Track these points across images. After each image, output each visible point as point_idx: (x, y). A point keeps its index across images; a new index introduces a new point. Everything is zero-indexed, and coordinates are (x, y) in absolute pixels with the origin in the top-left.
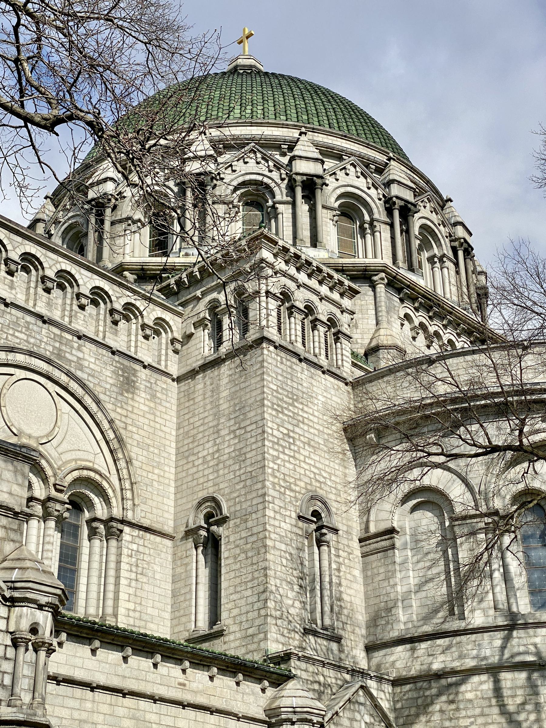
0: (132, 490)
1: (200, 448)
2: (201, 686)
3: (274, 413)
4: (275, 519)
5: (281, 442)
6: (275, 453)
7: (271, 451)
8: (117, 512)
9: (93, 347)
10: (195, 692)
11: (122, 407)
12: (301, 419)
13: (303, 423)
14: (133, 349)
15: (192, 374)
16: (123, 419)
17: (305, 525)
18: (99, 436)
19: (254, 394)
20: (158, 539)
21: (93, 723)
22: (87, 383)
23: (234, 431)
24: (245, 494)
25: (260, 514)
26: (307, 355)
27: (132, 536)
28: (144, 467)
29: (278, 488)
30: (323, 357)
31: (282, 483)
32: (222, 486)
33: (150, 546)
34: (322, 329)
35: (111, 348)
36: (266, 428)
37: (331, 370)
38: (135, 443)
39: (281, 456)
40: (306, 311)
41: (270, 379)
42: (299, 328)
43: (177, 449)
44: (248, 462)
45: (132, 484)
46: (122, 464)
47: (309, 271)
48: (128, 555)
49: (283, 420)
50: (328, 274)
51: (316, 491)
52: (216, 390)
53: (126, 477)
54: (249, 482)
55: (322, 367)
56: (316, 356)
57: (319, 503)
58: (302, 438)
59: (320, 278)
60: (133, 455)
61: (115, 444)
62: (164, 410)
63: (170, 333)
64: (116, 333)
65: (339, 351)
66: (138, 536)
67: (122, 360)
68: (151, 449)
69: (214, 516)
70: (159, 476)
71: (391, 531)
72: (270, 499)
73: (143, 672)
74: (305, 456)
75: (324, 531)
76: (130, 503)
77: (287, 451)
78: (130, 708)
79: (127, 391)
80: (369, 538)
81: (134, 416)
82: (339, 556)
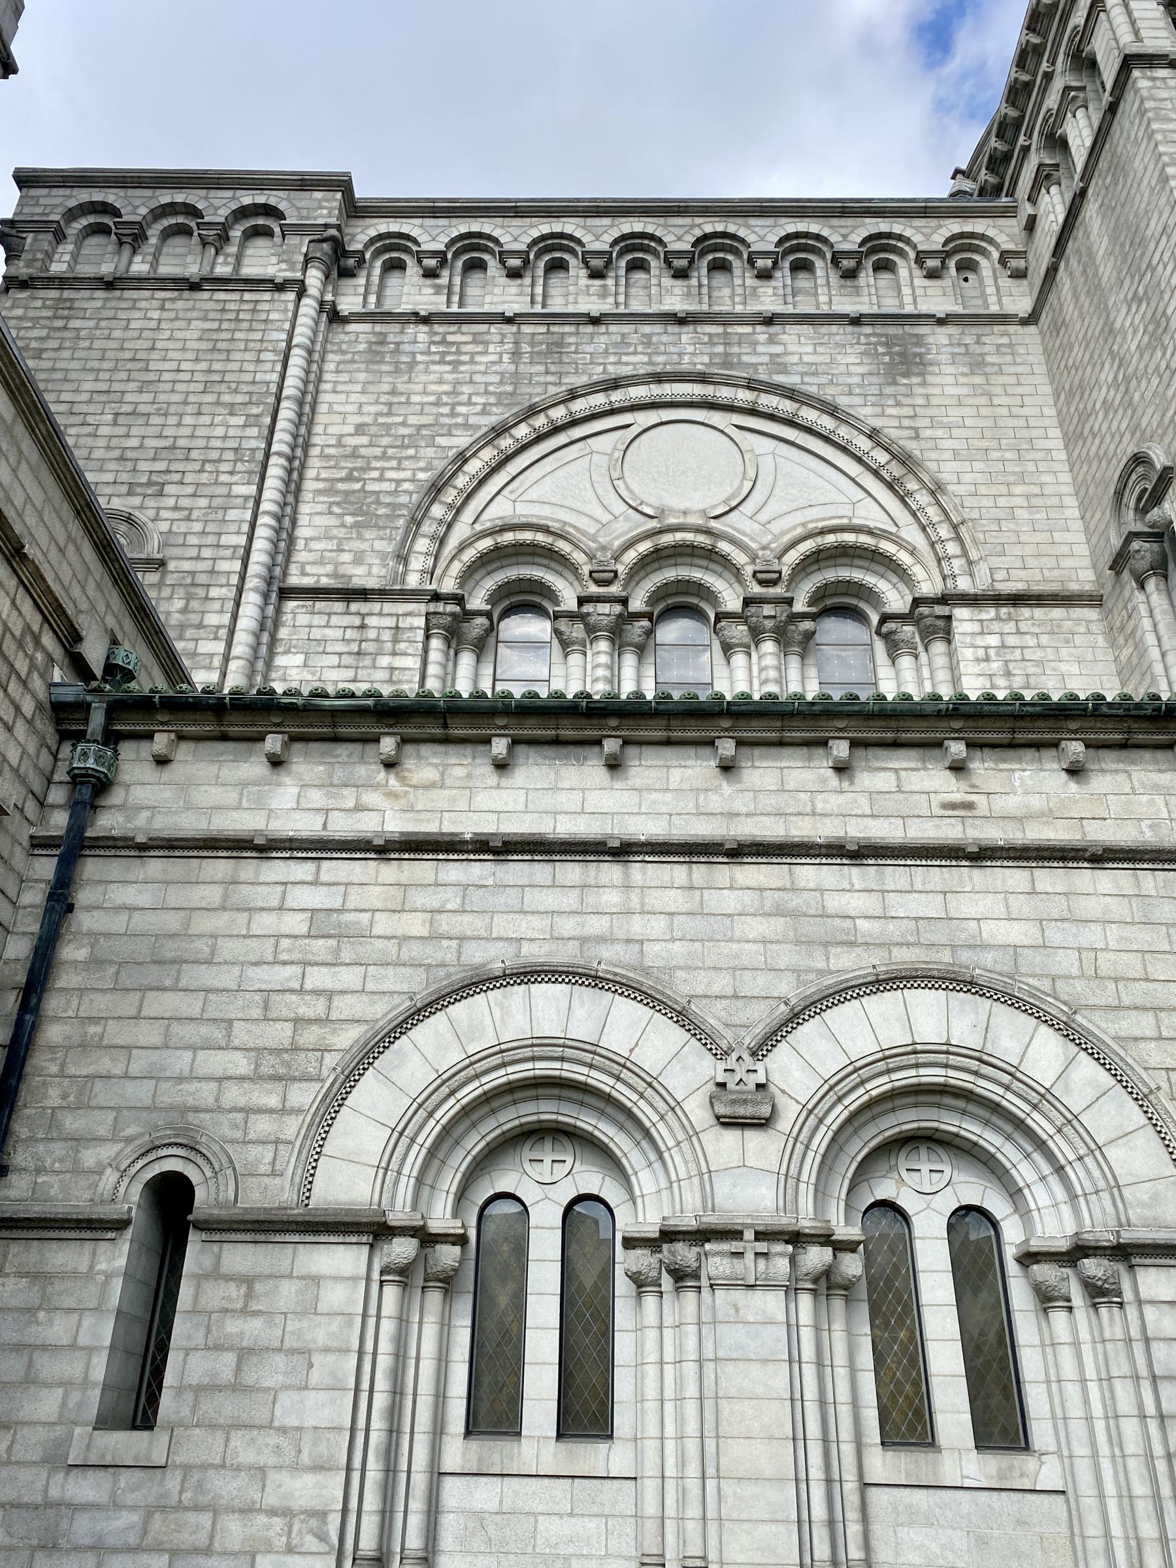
0: (958, 538)
2: (1036, 803)
8: (929, 586)
9: (806, 329)
10: (1020, 820)
11: (898, 404)
16: (906, 423)
18: (853, 468)
20: (1057, 613)
21: (628, 941)
27: (981, 621)
33: (1037, 630)
38: (948, 455)
45: (955, 527)
48: (977, 660)
53: (935, 519)
60: (945, 477)
61: (896, 470)
63: (990, 248)
67: (879, 330)
70: (1027, 497)
73: (802, 795)
78: (761, 890)
79: (906, 375)
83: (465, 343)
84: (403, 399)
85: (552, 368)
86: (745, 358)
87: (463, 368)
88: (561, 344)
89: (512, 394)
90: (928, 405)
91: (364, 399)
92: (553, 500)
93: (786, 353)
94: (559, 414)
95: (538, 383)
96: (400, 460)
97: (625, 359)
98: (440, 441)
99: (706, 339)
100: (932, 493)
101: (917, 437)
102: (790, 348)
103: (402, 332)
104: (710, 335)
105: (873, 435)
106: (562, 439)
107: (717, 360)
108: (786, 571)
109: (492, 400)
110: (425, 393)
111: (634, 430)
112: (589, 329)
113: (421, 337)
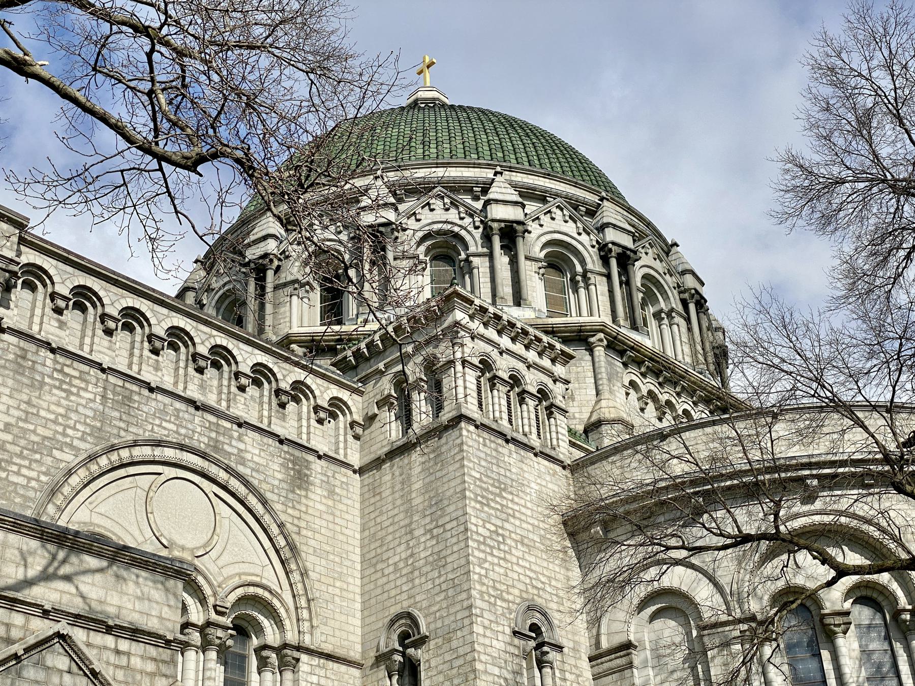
1: (390, 553)
3: (478, 506)
4: (484, 636)
5: (489, 541)
6: (482, 555)
7: (476, 553)
9: (256, 436)
11: (294, 508)
12: (511, 512)
13: (514, 517)
14: (304, 437)
15: (377, 463)
16: (296, 521)
17: (522, 642)
19: (453, 484)
20: (343, 668)
22: (251, 479)
23: (431, 531)
24: (447, 607)
25: (466, 631)
26: (515, 435)
28: (323, 579)
29: (486, 598)
30: (534, 436)
31: (491, 592)
32: (418, 598)
34: (532, 403)
35: (279, 436)
36: (469, 525)
37: (544, 451)
38: (311, 551)
39: (489, 558)
40: (511, 382)
41: (471, 465)
42: (504, 402)
43: (363, 555)
44: (449, 567)
45: (309, 601)
46: (296, 577)
47: (513, 334)
49: (490, 515)
50: (535, 336)
51: (533, 600)
52: (406, 482)
54: (451, 593)
55: (533, 449)
56: (526, 435)
57: (538, 615)
58: (513, 535)
59: (526, 342)
61: (286, 553)
62: (345, 508)
63: (348, 415)
64: (283, 418)
65: (553, 428)
66: (319, 666)
67: (291, 450)
68: (331, 557)
69: (410, 634)
71: (627, 647)
72: (478, 611)
74: (518, 558)
75: (545, 649)
76: (307, 624)
77: (495, 552)
79: (300, 488)
80: (600, 656)
81: (308, 518)
82: (565, 680)
83: (75, 377)
84: (35, 411)
85: (124, 417)
86: (226, 447)
87: (73, 398)
88: (130, 399)
89: (100, 429)
90: (306, 513)
91: (11, 402)
92: (113, 517)
93: (246, 451)
94: (125, 454)
95: (115, 426)
96: (31, 461)
97: (164, 424)
98: (56, 453)
99: (207, 425)
100: (302, 574)
101: (299, 533)
102: (249, 448)
103: (37, 353)
104: (210, 422)
105: (281, 526)
106: (122, 472)
107: (211, 443)
108: (229, 605)
109: (88, 431)
110: (48, 410)
111: (162, 478)
112: (146, 392)
113: (49, 363)
